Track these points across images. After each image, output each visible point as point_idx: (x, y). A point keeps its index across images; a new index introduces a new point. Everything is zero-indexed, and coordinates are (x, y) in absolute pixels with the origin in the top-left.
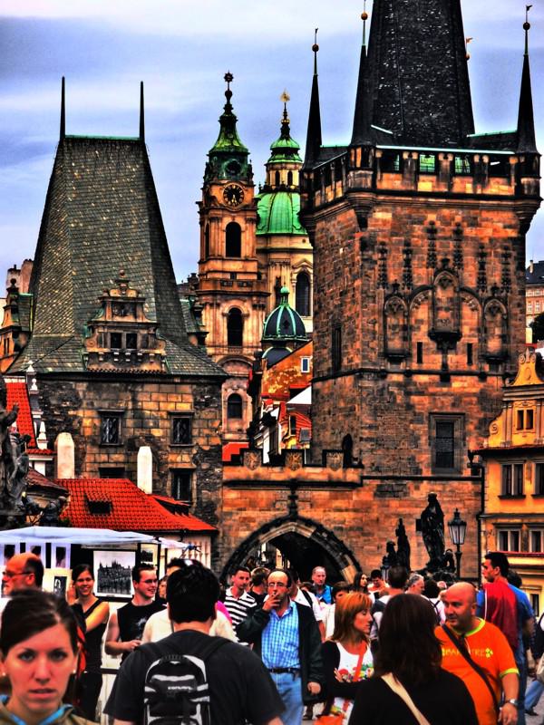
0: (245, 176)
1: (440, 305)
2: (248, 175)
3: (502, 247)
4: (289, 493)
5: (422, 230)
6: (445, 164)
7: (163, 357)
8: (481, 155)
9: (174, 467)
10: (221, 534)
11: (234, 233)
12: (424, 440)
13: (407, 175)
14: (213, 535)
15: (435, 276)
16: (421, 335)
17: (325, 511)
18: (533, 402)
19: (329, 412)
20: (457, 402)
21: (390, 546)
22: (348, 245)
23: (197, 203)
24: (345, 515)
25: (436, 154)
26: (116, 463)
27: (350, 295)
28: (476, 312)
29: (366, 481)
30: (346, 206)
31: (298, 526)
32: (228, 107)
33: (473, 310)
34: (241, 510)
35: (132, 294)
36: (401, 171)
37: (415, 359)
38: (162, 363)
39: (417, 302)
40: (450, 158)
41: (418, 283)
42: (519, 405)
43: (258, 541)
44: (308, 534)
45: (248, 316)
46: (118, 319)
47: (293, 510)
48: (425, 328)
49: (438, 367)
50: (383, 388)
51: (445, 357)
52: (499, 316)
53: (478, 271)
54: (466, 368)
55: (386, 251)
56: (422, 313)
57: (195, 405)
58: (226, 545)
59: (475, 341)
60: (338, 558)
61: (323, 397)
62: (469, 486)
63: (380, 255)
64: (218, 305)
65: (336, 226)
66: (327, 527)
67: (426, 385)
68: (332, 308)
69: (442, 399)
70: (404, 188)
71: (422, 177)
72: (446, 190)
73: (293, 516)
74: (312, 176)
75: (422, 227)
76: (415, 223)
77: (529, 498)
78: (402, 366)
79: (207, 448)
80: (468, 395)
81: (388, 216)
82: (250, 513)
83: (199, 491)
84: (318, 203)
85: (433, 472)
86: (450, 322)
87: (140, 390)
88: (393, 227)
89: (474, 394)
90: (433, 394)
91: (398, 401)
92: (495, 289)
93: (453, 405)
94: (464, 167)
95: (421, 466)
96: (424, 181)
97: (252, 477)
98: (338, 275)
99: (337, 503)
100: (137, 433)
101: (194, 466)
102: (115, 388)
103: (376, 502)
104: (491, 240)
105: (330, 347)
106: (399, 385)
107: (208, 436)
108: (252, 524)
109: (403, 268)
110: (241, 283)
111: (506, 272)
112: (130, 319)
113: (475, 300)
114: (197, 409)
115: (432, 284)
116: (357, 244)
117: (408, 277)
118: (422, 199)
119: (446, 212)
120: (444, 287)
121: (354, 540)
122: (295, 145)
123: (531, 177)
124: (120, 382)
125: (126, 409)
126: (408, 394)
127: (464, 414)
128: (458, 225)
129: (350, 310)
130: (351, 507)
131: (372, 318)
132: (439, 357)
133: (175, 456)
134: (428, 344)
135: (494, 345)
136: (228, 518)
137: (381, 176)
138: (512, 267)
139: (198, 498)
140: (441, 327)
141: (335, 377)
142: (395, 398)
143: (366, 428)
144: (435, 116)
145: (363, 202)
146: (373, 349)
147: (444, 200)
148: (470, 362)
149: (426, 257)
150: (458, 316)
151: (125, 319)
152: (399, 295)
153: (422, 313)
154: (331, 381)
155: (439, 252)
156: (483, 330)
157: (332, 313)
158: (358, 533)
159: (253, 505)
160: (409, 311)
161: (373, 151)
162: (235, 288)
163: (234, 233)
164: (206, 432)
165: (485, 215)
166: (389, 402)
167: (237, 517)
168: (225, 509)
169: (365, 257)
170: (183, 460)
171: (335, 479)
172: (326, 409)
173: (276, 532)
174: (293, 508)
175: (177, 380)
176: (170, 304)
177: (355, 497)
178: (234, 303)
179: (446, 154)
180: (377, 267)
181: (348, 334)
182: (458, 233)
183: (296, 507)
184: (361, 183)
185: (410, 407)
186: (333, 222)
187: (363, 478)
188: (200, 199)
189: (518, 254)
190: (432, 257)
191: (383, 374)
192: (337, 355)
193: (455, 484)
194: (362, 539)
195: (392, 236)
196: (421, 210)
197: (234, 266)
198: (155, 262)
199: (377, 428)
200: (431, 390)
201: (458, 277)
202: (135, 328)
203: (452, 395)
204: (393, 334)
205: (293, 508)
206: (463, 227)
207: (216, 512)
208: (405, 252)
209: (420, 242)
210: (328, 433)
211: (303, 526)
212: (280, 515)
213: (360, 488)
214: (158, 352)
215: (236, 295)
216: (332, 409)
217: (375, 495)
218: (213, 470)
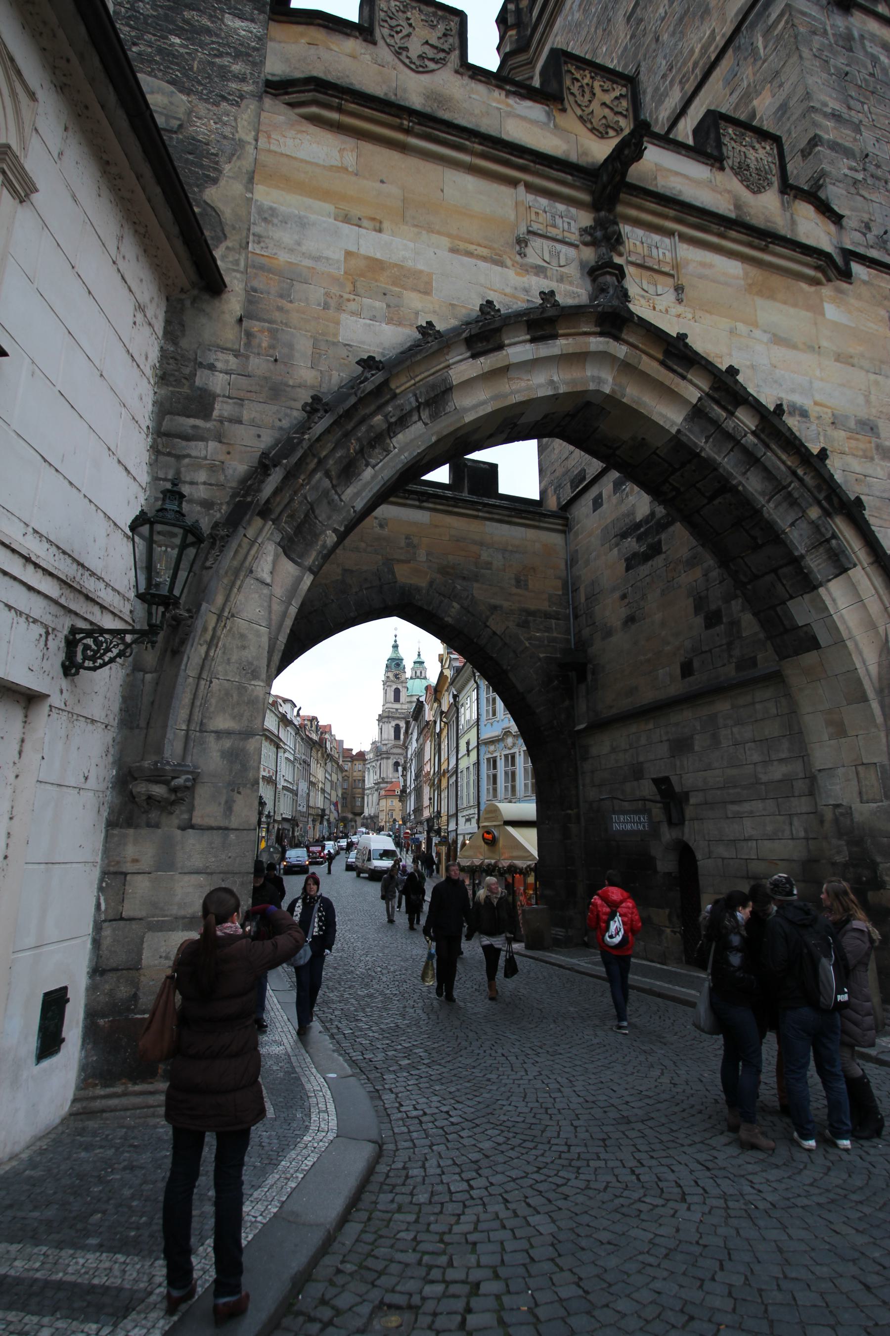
10: (233, 303)
11: (397, 692)
17: (732, 332)
29: (857, 268)
34: (347, 219)
44: (670, 417)
58: (258, 365)
60: (798, 538)
66: (749, 381)
82: (397, 246)
97: (416, 101)
99: (781, 313)
108: (413, 301)
143: (825, 115)
163: (397, 692)
166: (872, 75)
178: (397, 722)
197: (397, 706)
199: (857, 128)
207: (211, 194)
213: (845, 286)
215: (398, 718)
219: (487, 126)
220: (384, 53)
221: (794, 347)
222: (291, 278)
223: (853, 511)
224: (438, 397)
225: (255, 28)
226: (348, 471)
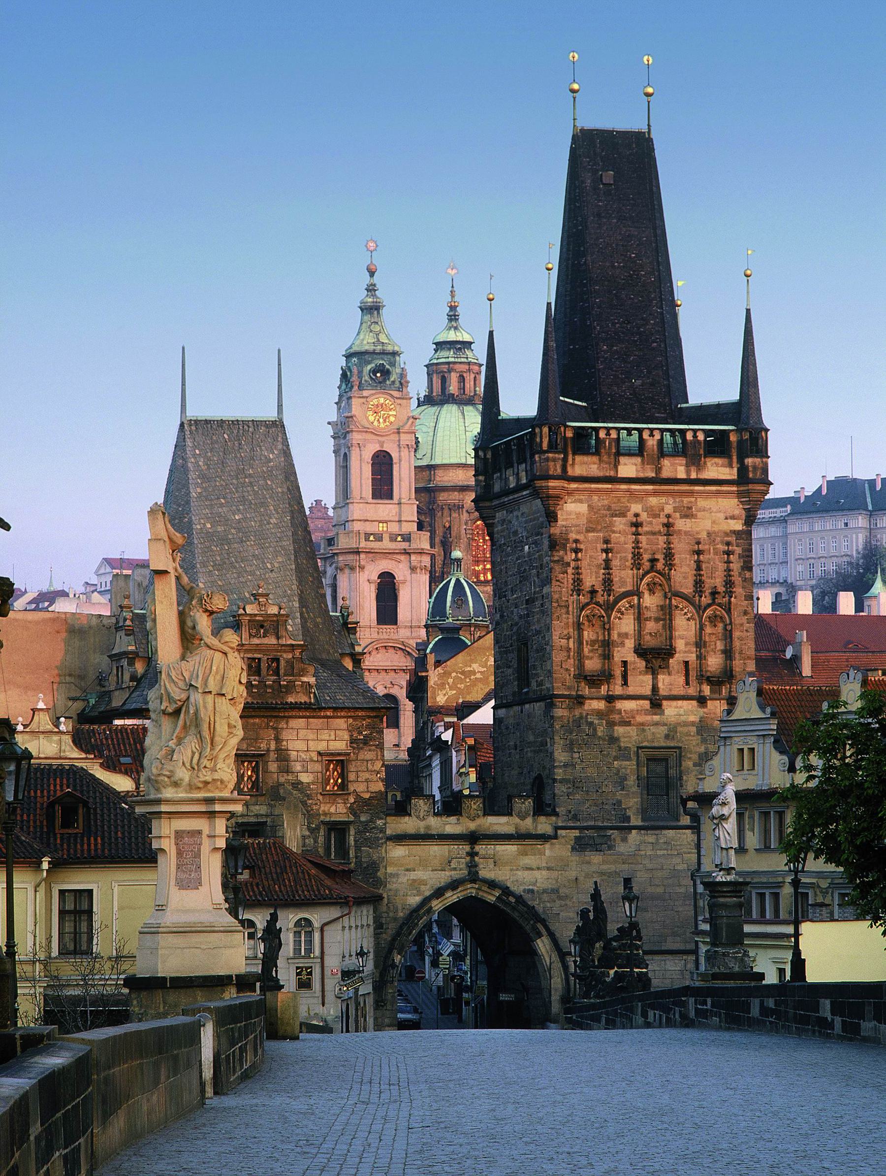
0: (397, 384)
1: (648, 614)
2: (401, 384)
3: (722, 542)
4: (467, 848)
5: (625, 524)
6: (651, 443)
7: (310, 686)
8: (695, 431)
9: (328, 819)
10: (386, 900)
12: (632, 780)
13: (605, 458)
14: (375, 900)
15: (641, 580)
16: (625, 652)
18: (755, 739)
19: (516, 746)
20: (672, 733)
21: (584, 914)
22: (535, 543)
23: (329, 423)
24: (537, 874)
25: (640, 431)
26: (257, 816)
27: (538, 603)
28: (692, 623)
29: (559, 832)
30: (530, 495)
31: (478, 889)
32: (371, 289)
33: (688, 619)
35: (273, 610)
36: (597, 453)
37: (619, 681)
38: (310, 693)
39: (619, 611)
40: (657, 436)
41: (619, 589)
42: (738, 742)
43: (431, 907)
44: (491, 899)
45: (404, 582)
46: (256, 641)
47: (473, 870)
48: (630, 644)
49: (647, 691)
50: (581, 717)
51: (655, 679)
52: (721, 625)
53: (695, 572)
54: (681, 692)
55: (581, 550)
56: (626, 624)
57: (351, 743)
59: (692, 657)
60: (528, 928)
61: (507, 728)
62: (688, 836)
63: (574, 555)
64: (362, 568)
65: (520, 519)
67: (633, 713)
68: (516, 618)
69: (653, 729)
70: (601, 474)
71: (623, 460)
72: (654, 475)
73: (473, 877)
74: (489, 455)
75: (623, 520)
76: (616, 516)
77: (752, 852)
78: (604, 690)
79: (367, 796)
80: (686, 724)
81: (583, 508)
83: (358, 848)
84: (497, 488)
85: (643, 820)
86: (661, 635)
87: (285, 726)
88: (589, 521)
89: (693, 724)
90: (642, 724)
91: (600, 734)
92: (714, 593)
93: (667, 737)
94: (675, 443)
95: (629, 813)
96: (625, 464)
97: (422, 831)
98: (524, 578)
100: (282, 780)
101: (352, 818)
102: (254, 724)
103: (575, 858)
104: (709, 534)
105: (516, 666)
106: (599, 714)
107: (367, 781)
109: (603, 571)
110: (393, 538)
111: (729, 570)
112: (272, 640)
113: (691, 608)
114: (354, 748)
115: (638, 589)
116: (546, 543)
117: (608, 582)
118: (624, 487)
119: (653, 501)
120: (652, 591)
121: (548, 905)
122: (467, 338)
123: (756, 457)
124: (263, 717)
125: (268, 750)
126: (611, 724)
127: (680, 748)
128: (668, 516)
129: (538, 621)
130: (544, 865)
131: (565, 632)
132: (649, 678)
133: (329, 805)
134: (634, 663)
135: (714, 662)
136: (394, 880)
137: (574, 459)
138: (736, 566)
139: (356, 857)
140: (649, 642)
141: (522, 703)
142: (595, 730)
143: (560, 767)
144: (639, 382)
145: (551, 492)
146: (567, 670)
147: (651, 487)
148: (687, 683)
149: (630, 556)
150: (669, 627)
151: (266, 641)
152: (597, 604)
153: (626, 624)
154: (517, 708)
155: (646, 550)
156: (700, 644)
157: (517, 624)
158: (554, 896)
159: (423, 863)
160: (609, 622)
161: (562, 429)
162: (386, 544)
164: (367, 775)
165: (702, 503)
166: (587, 735)
167: (405, 880)
168: (390, 870)
169: (556, 558)
170: (338, 811)
171: (523, 830)
172: (512, 743)
173: (452, 897)
174: (472, 867)
175: (328, 714)
176: (319, 620)
177: (548, 853)
179: (652, 430)
180: (570, 570)
181: (537, 651)
182: (668, 525)
183: (476, 866)
184: (548, 470)
185: (613, 740)
186: (515, 513)
187: (557, 828)
188: (334, 418)
189: (744, 550)
190: (637, 556)
191: (580, 700)
192: (524, 675)
193: (671, 833)
194: (558, 902)
195: (588, 531)
196: (623, 500)
198: (299, 570)
199: (574, 766)
200: (639, 719)
201: (670, 579)
202: (278, 651)
203: (666, 725)
204: (592, 651)
205: (472, 867)
206: (676, 519)
208: (604, 550)
209: (622, 539)
210: (515, 772)
211: (485, 888)
212: (457, 877)
214: (305, 679)
216: (518, 743)
217: (573, 849)
218: (375, 823)
219: (440, 831)
220: (415, 818)
221: (533, 869)
222: (397, 890)
223: (544, 922)
224: (430, 911)
225: (383, 821)
226: (410, 934)
